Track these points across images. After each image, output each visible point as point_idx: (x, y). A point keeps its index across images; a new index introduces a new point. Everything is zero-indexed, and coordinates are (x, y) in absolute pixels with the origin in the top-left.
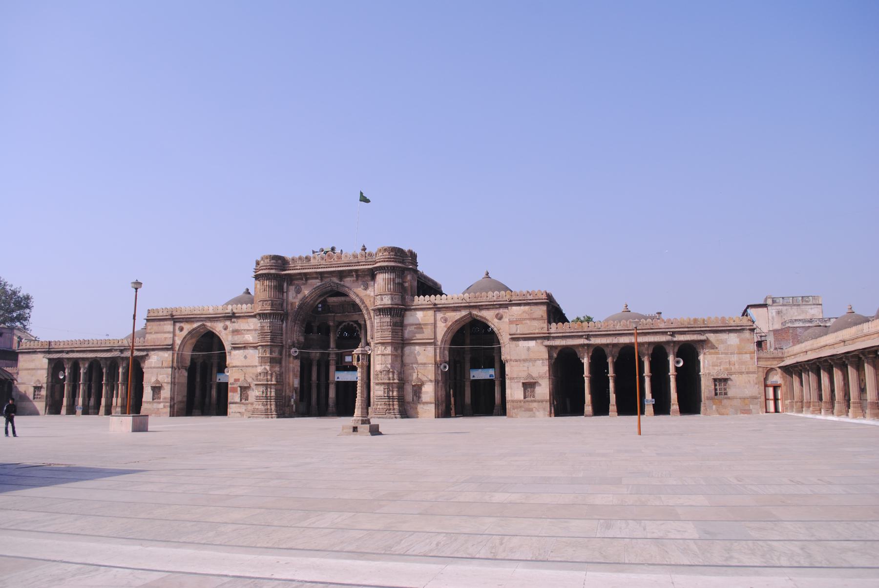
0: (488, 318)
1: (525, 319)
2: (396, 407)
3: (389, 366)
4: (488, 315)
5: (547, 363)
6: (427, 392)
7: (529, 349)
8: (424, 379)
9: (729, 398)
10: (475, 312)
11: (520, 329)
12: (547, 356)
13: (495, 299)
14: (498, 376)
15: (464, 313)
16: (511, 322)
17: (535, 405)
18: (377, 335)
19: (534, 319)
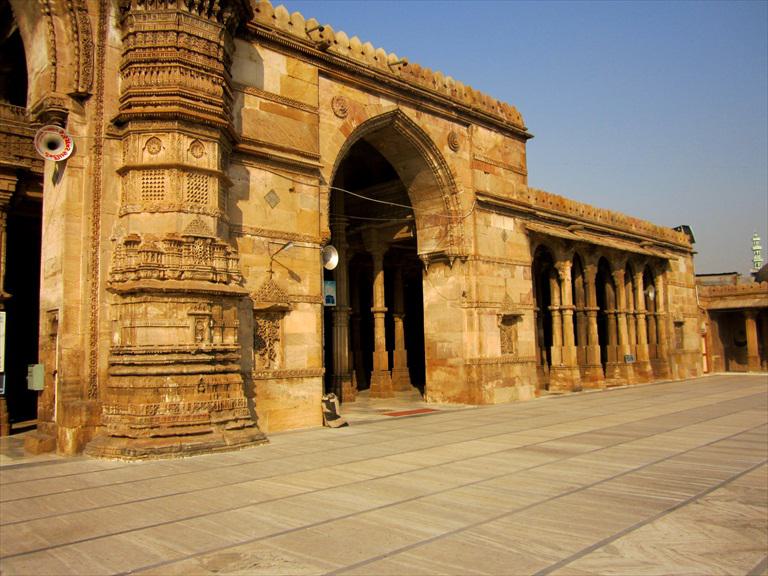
0: (435, 138)
1: (497, 164)
2: (238, 395)
3: (211, 223)
4: (435, 128)
5: (529, 271)
6: (299, 338)
7: (504, 236)
8: (293, 288)
9: (684, 353)
10: (409, 112)
11: (488, 184)
12: (527, 257)
13: (448, 92)
14: (345, 300)
15: (386, 105)
16: (476, 164)
17: (517, 369)
18: (116, 84)
19: (510, 169)
